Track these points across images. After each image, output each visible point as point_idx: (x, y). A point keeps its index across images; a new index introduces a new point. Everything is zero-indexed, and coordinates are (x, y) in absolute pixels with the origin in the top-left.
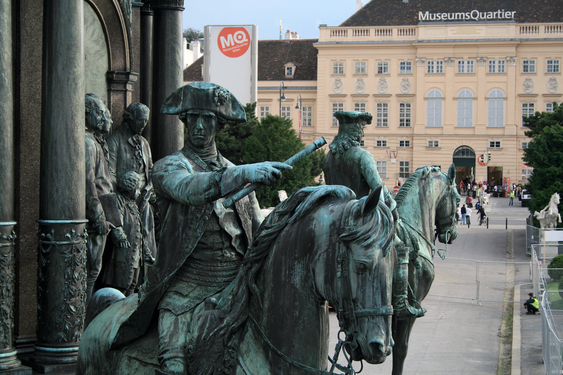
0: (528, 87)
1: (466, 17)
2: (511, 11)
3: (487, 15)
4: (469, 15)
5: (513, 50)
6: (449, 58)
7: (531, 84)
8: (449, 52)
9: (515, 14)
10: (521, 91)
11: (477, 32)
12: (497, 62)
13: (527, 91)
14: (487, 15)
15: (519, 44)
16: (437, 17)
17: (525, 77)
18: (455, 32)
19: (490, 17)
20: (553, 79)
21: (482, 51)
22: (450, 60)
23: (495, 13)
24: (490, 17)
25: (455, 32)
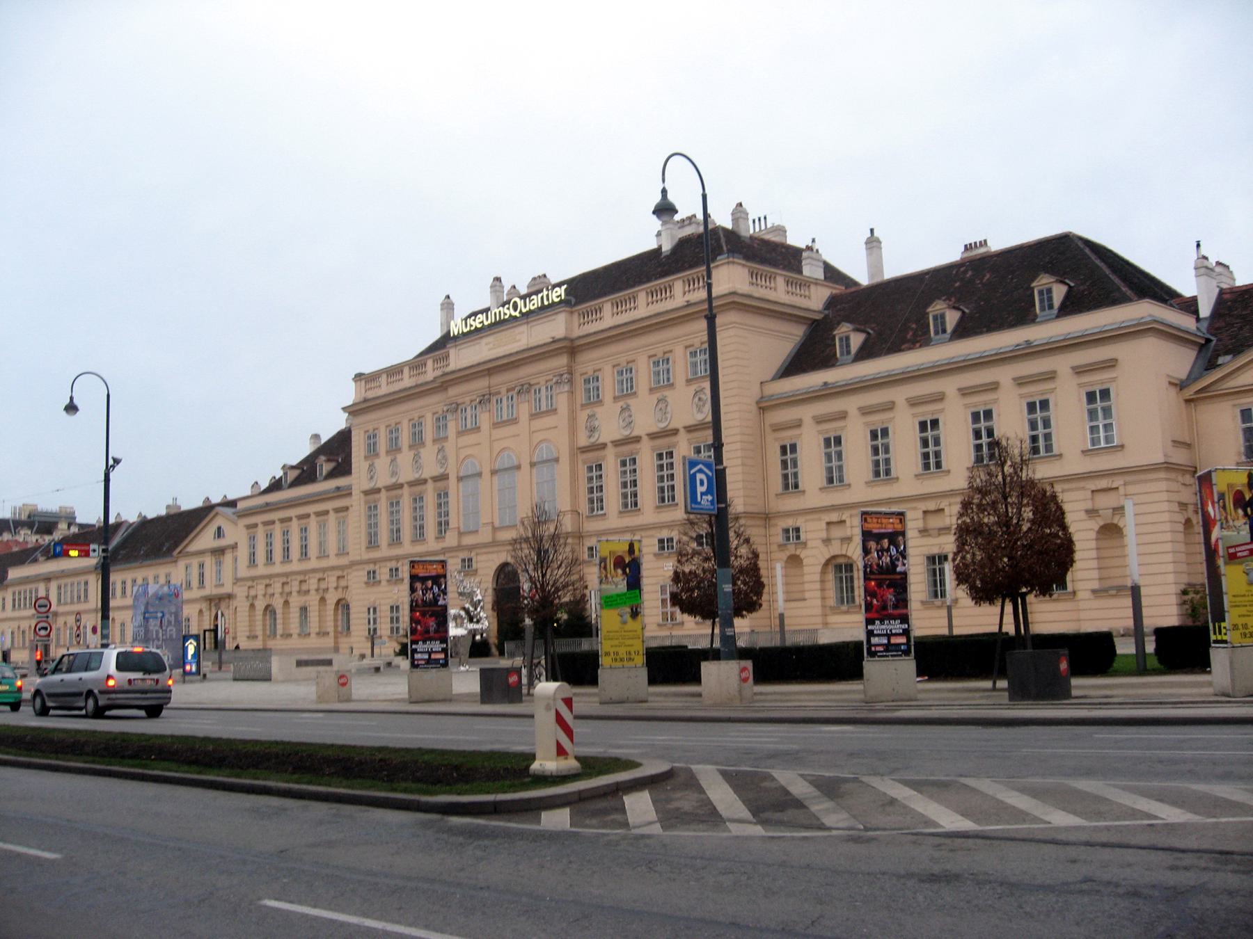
0: (592, 430)
1: (505, 314)
2: (560, 287)
3: (530, 301)
4: (508, 309)
5: (563, 361)
6: (484, 396)
7: (597, 423)
8: (481, 384)
9: (566, 290)
10: (583, 441)
11: (518, 338)
12: (543, 389)
13: (592, 440)
14: (530, 301)
15: (571, 348)
16: (471, 326)
17: (588, 411)
18: (491, 346)
19: (534, 305)
20: (625, 406)
21: (524, 372)
22: (485, 400)
23: (540, 296)
24: (534, 305)
25: (491, 346)
